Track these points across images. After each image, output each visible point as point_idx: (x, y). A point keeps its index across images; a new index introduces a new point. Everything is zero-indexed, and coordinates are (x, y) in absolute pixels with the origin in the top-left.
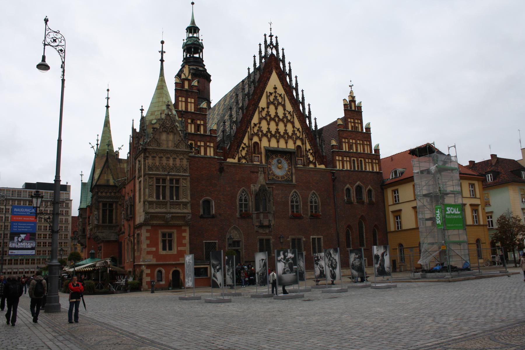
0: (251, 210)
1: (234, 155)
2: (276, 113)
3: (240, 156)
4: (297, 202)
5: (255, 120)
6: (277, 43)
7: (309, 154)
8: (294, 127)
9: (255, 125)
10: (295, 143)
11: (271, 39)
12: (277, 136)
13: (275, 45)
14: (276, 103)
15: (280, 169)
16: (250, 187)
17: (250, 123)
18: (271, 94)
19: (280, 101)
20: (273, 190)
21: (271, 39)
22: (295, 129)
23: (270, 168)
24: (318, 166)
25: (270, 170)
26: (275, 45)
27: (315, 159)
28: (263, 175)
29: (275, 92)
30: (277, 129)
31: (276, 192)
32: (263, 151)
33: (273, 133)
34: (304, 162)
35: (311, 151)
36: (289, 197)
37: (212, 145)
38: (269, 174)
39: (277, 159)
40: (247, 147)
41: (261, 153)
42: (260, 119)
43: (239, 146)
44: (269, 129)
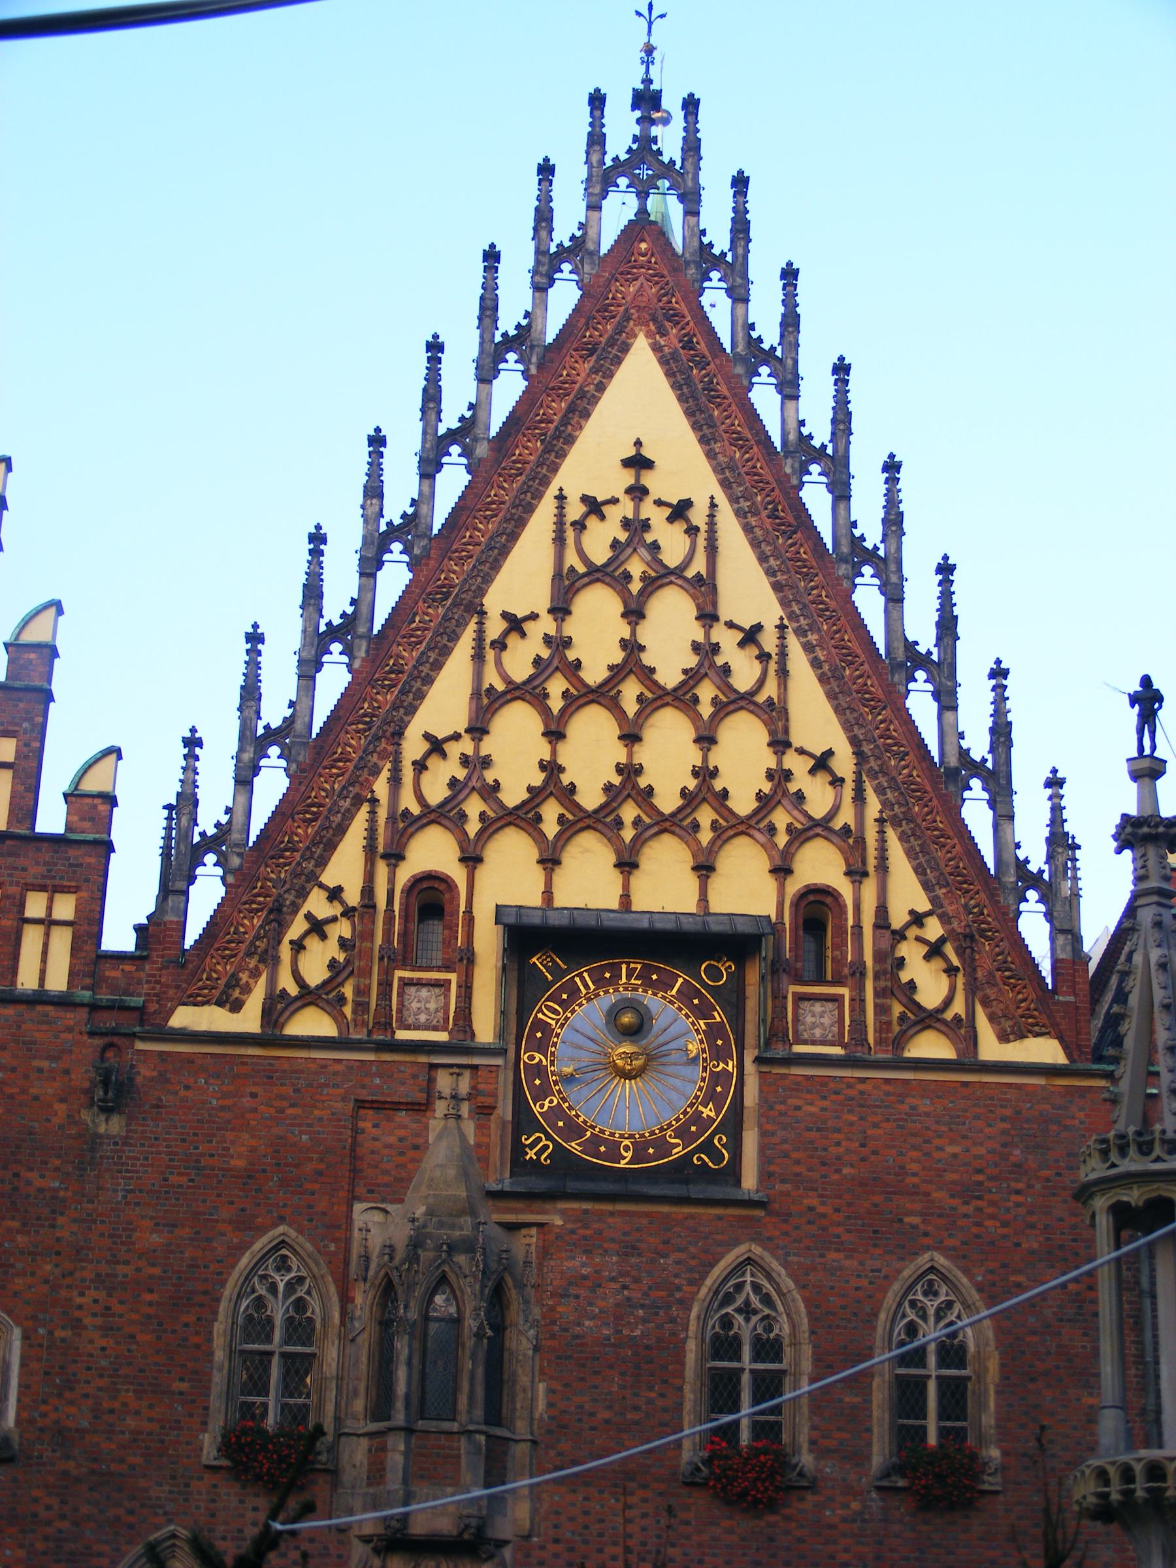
0: (330, 1408)
1: (233, 982)
2: (632, 647)
4: (767, 1348)
5: (445, 705)
6: (692, 146)
7: (911, 952)
8: (780, 744)
9: (436, 746)
10: (782, 870)
11: (646, 121)
12: (626, 816)
14: (636, 567)
15: (632, 1084)
16: (339, 1228)
17: (399, 734)
18: (594, 507)
19: (672, 556)
20: (545, 1252)
22: (792, 761)
24: (991, 1048)
27: (972, 990)
28: (469, 1128)
29: (638, 492)
30: (630, 771)
31: (578, 1264)
33: (590, 798)
34: (859, 1025)
36: (685, 1304)
37: (65, 908)
38: (523, 1121)
39: (609, 999)
40: (348, 912)
41: (467, 959)
42: (486, 706)
43: (279, 917)
44: (552, 768)
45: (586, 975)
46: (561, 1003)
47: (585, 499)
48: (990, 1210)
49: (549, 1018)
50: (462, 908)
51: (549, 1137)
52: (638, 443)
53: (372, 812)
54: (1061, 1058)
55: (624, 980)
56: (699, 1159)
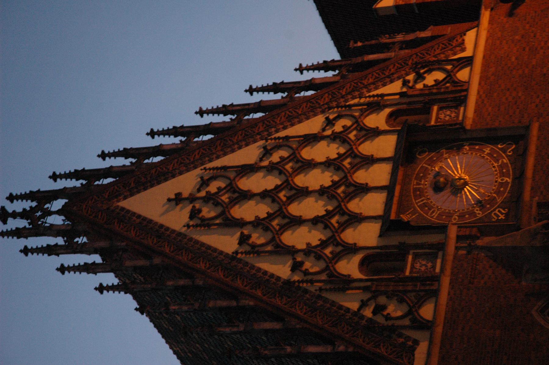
3: (407, 322)
11: (14, 215)
13: (34, 204)
17: (288, 283)
21: (14, 215)
22: (328, 132)
23: (461, 216)
25: (472, 214)
26: (34, 204)
29: (192, 199)
32: (395, 240)
35: (411, 77)
45: (417, 201)
46: (429, 209)
47: (191, 217)
48: (543, 44)
49: (435, 215)
50: (379, 251)
51: (495, 210)
52: (169, 200)
53: (326, 290)
54: (475, 29)
55: (422, 186)
56: (510, 152)
